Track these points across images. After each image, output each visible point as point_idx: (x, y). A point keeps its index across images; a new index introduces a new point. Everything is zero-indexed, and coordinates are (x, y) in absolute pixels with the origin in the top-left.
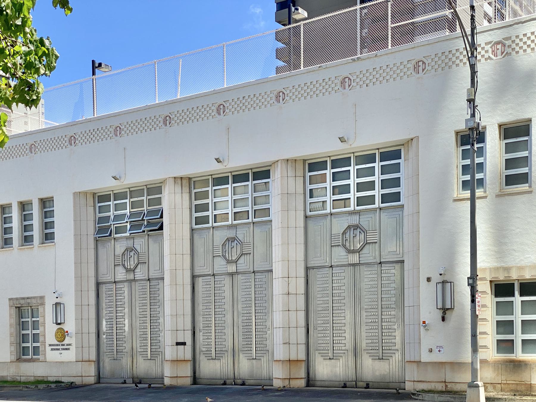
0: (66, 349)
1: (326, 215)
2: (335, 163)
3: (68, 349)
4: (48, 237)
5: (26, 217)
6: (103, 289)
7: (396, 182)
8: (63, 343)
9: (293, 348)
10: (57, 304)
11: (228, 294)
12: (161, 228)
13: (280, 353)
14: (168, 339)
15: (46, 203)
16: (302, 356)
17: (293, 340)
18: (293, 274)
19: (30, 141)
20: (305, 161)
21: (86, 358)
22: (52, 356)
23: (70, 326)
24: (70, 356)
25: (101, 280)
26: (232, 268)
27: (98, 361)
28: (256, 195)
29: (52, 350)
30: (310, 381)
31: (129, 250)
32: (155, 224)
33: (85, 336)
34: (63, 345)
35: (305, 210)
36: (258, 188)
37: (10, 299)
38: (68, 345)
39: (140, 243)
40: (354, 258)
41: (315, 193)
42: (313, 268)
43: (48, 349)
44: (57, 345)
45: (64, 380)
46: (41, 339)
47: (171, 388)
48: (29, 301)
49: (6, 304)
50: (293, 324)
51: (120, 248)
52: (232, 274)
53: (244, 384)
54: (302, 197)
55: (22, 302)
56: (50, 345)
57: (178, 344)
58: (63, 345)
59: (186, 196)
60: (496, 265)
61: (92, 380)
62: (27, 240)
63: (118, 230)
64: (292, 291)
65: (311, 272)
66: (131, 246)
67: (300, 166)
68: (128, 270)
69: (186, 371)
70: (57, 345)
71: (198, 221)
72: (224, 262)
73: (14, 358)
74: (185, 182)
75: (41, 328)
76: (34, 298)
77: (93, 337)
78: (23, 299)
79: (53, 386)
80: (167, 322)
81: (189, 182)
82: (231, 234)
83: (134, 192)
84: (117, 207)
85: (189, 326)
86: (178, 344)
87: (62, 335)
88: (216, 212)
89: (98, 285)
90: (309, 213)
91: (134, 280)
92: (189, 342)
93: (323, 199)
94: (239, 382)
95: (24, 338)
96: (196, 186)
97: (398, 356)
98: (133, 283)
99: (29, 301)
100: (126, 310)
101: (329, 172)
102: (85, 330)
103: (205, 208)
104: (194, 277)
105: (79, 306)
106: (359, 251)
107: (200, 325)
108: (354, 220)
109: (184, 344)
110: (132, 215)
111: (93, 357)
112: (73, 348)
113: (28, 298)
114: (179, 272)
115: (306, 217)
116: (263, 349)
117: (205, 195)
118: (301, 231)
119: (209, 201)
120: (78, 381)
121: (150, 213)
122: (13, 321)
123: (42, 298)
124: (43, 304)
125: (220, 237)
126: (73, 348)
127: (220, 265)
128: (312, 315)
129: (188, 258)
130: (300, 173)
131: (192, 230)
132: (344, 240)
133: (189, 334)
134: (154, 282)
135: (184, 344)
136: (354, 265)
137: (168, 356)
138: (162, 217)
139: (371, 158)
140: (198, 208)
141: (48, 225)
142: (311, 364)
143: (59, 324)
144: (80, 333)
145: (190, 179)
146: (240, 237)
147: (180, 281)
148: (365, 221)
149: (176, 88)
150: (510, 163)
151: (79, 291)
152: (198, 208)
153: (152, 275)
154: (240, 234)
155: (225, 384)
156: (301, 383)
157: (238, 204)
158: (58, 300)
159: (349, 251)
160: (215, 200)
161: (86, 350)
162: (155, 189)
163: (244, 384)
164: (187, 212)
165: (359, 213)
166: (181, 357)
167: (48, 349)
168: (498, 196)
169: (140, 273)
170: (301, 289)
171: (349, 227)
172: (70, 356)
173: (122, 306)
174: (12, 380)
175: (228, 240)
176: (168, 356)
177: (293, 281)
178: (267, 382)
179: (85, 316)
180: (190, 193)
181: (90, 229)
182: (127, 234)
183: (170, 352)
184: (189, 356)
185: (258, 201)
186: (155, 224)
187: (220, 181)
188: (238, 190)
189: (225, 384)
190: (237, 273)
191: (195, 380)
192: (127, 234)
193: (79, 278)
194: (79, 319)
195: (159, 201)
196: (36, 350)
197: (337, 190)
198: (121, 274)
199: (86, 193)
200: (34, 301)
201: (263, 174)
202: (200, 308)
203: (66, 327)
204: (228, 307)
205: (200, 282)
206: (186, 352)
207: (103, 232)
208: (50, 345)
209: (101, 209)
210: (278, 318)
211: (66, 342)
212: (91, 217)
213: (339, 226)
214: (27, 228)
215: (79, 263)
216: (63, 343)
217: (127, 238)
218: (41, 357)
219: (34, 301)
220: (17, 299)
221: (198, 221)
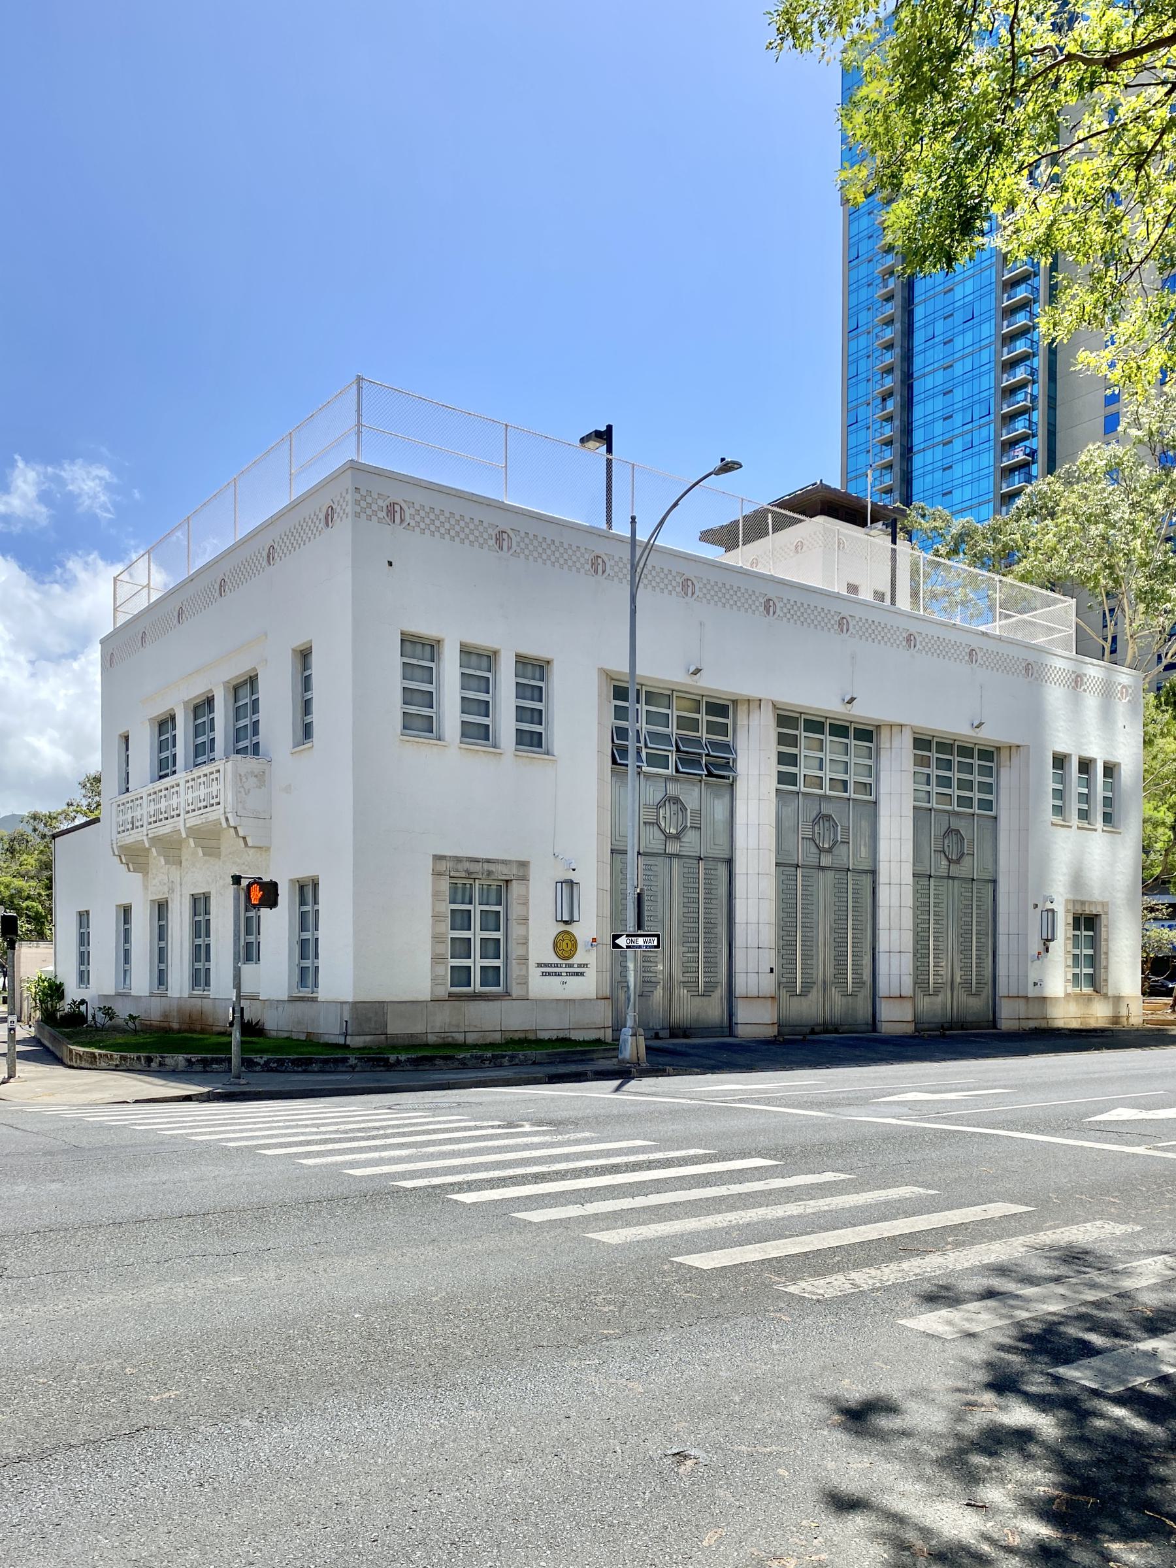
0: (577, 974)
3: (582, 974)
8: (570, 962)
23: (587, 927)
24: (586, 986)
29: (544, 974)
34: (570, 966)
37: (438, 858)
38: (580, 966)
39: (691, 795)
43: (534, 973)
44: (556, 966)
45: (576, 1035)
48: (492, 867)
56: (540, 965)
58: (570, 966)
70: (556, 966)
76: (504, 862)
78: (476, 860)
87: (565, 945)
98: (675, 862)
99: (492, 867)
112: (591, 973)
113: (488, 861)
124: (524, 878)
126: (591, 973)
143: (566, 922)
172: (586, 986)
174: (440, 1041)
196: (491, 975)
208: (540, 965)
211: (576, 960)
216: (570, 962)
217: (667, 778)
220: (458, 859)
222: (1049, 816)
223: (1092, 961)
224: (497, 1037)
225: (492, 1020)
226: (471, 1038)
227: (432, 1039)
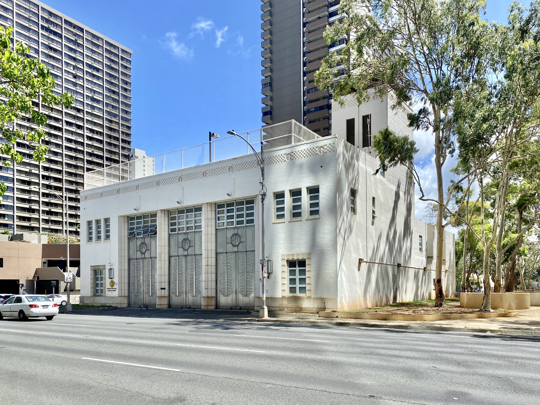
1: (224, 229)
2: (229, 205)
4: (108, 237)
5: (99, 227)
6: (132, 262)
7: (252, 215)
9: (210, 291)
10: (110, 269)
11: (184, 265)
12: (156, 233)
13: (204, 293)
14: (158, 287)
15: (107, 220)
16: (214, 295)
17: (210, 287)
18: (210, 256)
19: (100, 191)
20: (216, 204)
21: (123, 295)
22: (108, 294)
23: (116, 280)
24: (116, 294)
25: (131, 258)
26: (186, 253)
27: (129, 297)
28: (196, 219)
30: (217, 306)
31: (143, 243)
32: (153, 231)
33: (123, 285)
35: (216, 226)
36: (197, 215)
39: (147, 241)
40: (235, 249)
41: (220, 218)
42: (219, 253)
43: (107, 290)
46: (104, 286)
47: (158, 309)
49: (89, 268)
50: (210, 279)
51: (139, 243)
52: (186, 256)
53: (190, 308)
54: (214, 220)
55: (96, 268)
57: (162, 289)
59: (167, 219)
60: (289, 253)
61: (126, 306)
62: (99, 238)
63: (139, 234)
64: (210, 264)
65: (219, 255)
66: (143, 241)
67: (213, 206)
68: (142, 253)
69: (165, 302)
71: (173, 230)
72: (182, 250)
73: (92, 295)
74: (166, 212)
75: (104, 280)
77: (127, 285)
79: (106, 308)
80: (157, 278)
81: (169, 212)
82: (185, 237)
83: (145, 216)
84: (138, 223)
85: (167, 280)
86: (162, 289)
87: (112, 284)
88: (179, 227)
89: (129, 260)
90: (217, 228)
91: (145, 258)
92: (167, 288)
93: (223, 221)
94: (188, 307)
95: (97, 285)
96: (172, 213)
97: (252, 295)
100: (141, 273)
101: (225, 209)
102: (123, 281)
103: (174, 224)
104: (170, 257)
105: (120, 270)
106: (237, 246)
107: (172, 280)
108: (235, 231)
109: (164, 289)
110: (144, 227)
111: (126, 294)
112: (117, 290)
114: (163, 255)
115: (216, 230)
116: (198, 292)
117: (174, 218)
118: (214, 236)
119: (176, 221)
120: (119, 306)
121: (151, 226)
122: (92, 277)
123: (104, 266)
124: (105, 269)
125: (181, 238)
126: (117, 290)
127: (181, 252)
128: (219, 275)
129: (167, 248)
130: (214, 209)
131: (169, 235)
132: (231, 241)
133: (167, 284)
134: (153, 258)
135: (164, 289)
136: (235, 252)
137: (158, 295)
138: (156, 228)
139: (242, 203)
140: (173, 224)
141: (108, 231)
142: (218, 298)
144: (120, 283)
145: (168, 211)
146: (189, 238)
147: (163, 259)
148: (240, 232)
149: (162, 168)
150: (294, 208)
151: (120, 263)
152: (173, 224)
153: (153, 255)
154: (190, 237)
155: (182, 308)
156: (213, 308)
157: (189, 223)
158: (111, 267)
159: (234, 246)
160: (179, 221)
161: (123, 291)
162: (154, 215)
163: (190, 308)
164: (167, 226)
165: (237, 228)
166: (163, 294)
167: (107, 290)
168: (289, 222)
169: (147, 255)
170: (214, 263)
171: (233, 234)
173: (140, 270)
175: (184, 239)
176: (158, 295)
177: (210, 259)
178: (199, 307)
179: (123, 275)
180: (168, 217)
181: (126, 233)
182: (142, 236)
183: (159, 293)
184: (167, 294)
185: (197, 221)
186: (153, 231)
187: (181, 211)
188: (189, 216)
189: (182, 308)
190: (188, 255)
191: (169, 306)
192: (142, 236)
193: (120, 256)
194: (120, 277)
195: (155, 221)
197: (229, 217)
198: (139, 255)
199: (124, 216)
200: (101, 267)
201: (198, 209)
202: (172, 271)
203: (114, 280)
204: (184, 271)
205: (172, 259)
206: (165, 293)
207: (132, 235)
209: (131, 224)
210: (203, 277)
212: (126, 228)
213: (230, 234)
214: (99, 232)
215: (120, 250)
217: (142, 238)
218: (103, 294)
219: (101, 267)
220: (94, 266)
221: (173, 230)
222: (274, 219)
223: (97, 285)
224: (99, 305)
225: (100, 301)
226: (96, 305)
227: (90, 305)
